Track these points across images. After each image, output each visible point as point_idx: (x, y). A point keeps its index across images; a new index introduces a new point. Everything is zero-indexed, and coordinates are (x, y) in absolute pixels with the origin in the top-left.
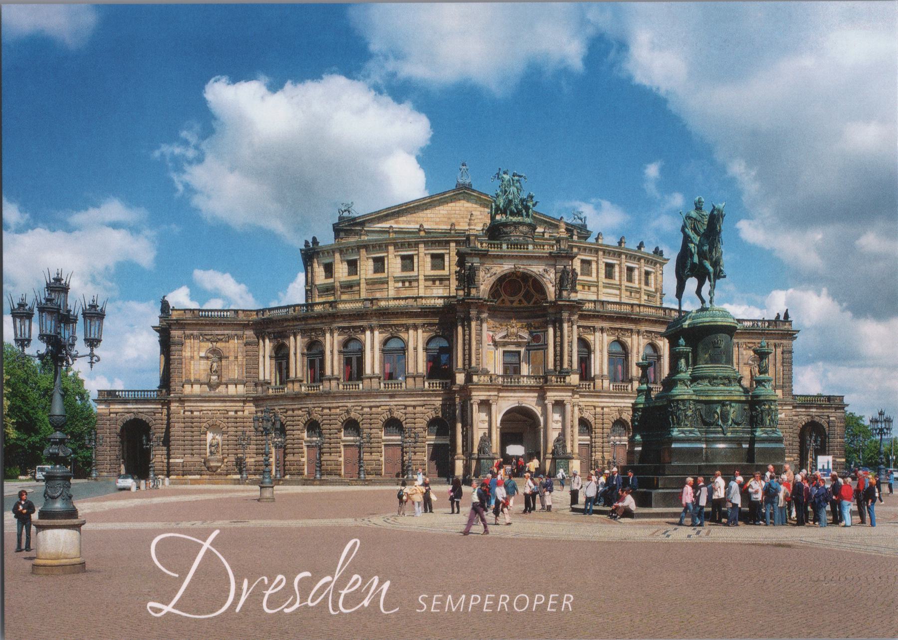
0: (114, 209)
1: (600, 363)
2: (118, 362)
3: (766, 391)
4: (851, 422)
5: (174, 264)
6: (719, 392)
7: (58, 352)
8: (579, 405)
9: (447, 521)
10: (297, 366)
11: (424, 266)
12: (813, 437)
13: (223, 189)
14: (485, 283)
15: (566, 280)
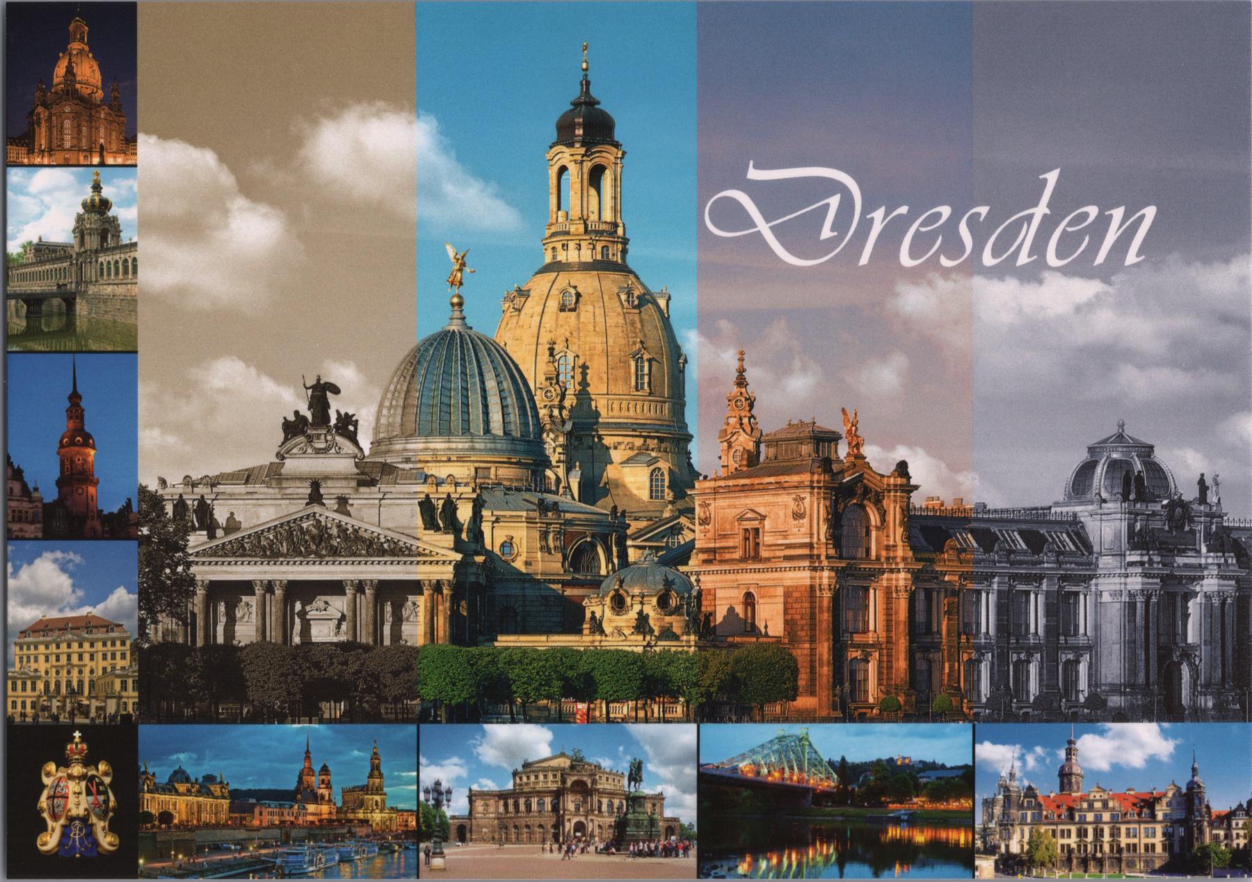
0: (455, 760)
1: (604, 808)
2: (456, 807)
3: (656, 816)
4: (682, 826)
5: (473, 777)
6: (641, 817)
7: (438, 804)
8: (598, 821)
9: (557, 856)
10: (511, 808)
11: (550, 777)
12: (670, 830)
13: (488, 754)
14: (569, 783)
15: (594, 782)
